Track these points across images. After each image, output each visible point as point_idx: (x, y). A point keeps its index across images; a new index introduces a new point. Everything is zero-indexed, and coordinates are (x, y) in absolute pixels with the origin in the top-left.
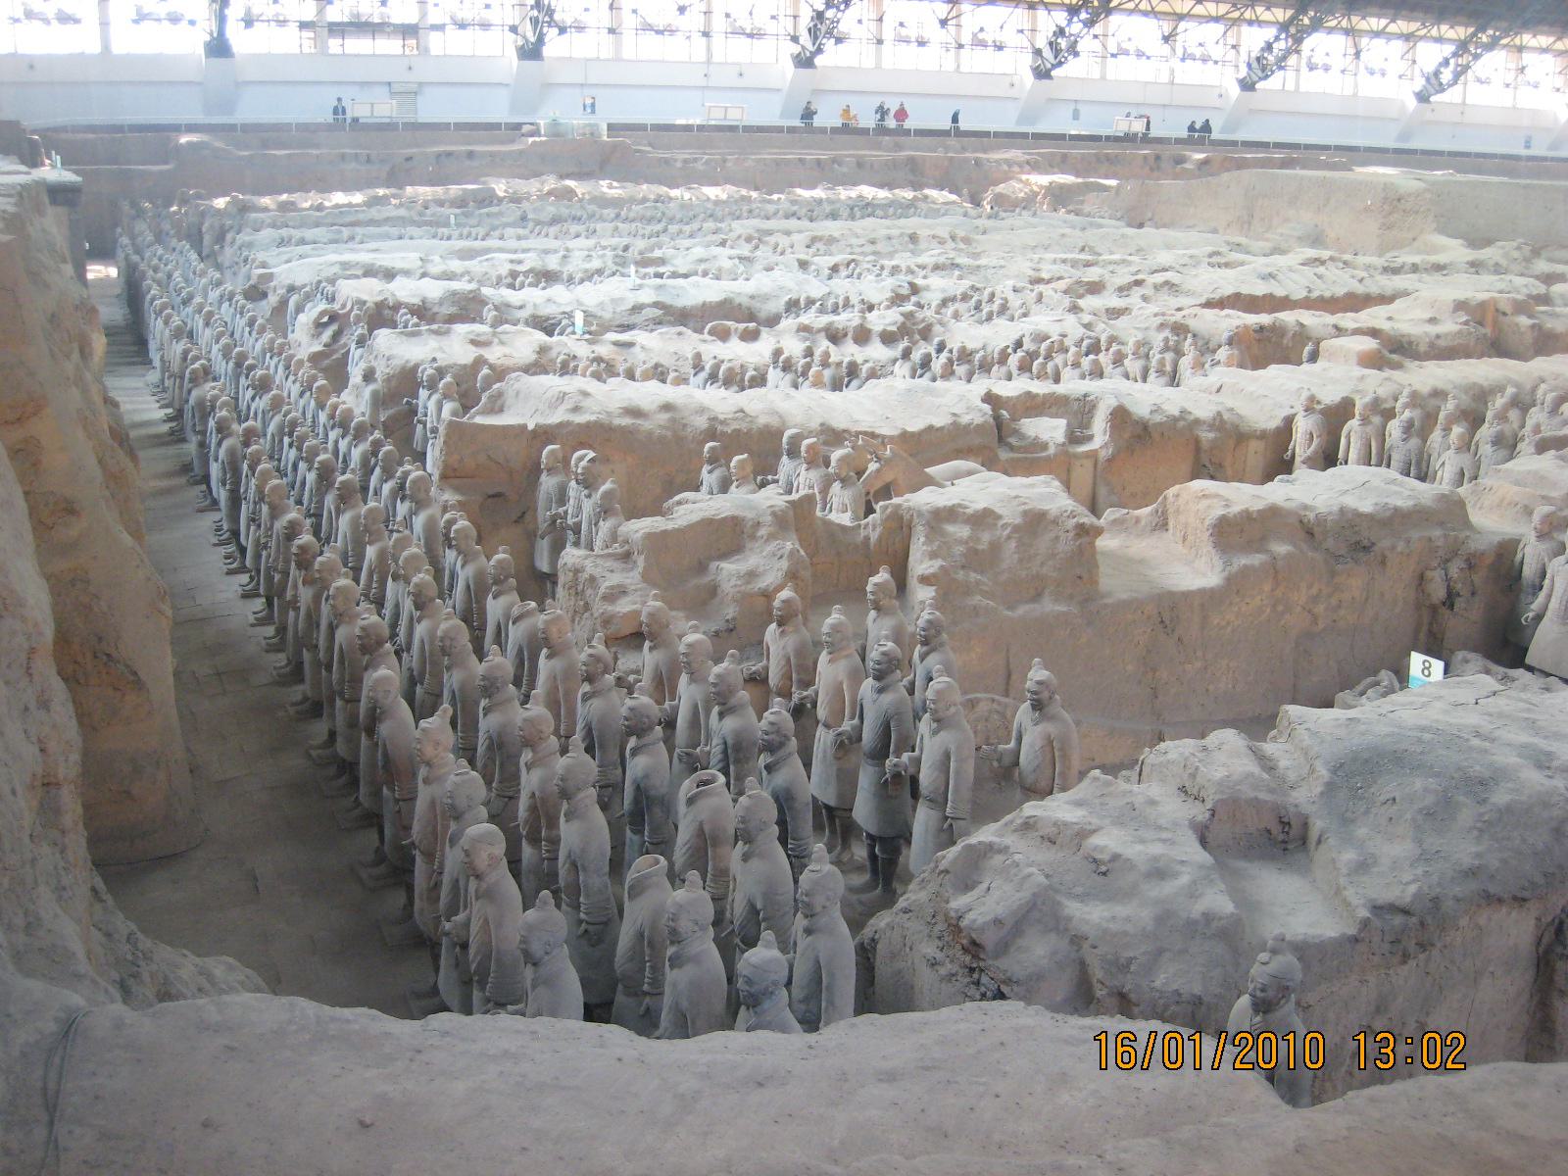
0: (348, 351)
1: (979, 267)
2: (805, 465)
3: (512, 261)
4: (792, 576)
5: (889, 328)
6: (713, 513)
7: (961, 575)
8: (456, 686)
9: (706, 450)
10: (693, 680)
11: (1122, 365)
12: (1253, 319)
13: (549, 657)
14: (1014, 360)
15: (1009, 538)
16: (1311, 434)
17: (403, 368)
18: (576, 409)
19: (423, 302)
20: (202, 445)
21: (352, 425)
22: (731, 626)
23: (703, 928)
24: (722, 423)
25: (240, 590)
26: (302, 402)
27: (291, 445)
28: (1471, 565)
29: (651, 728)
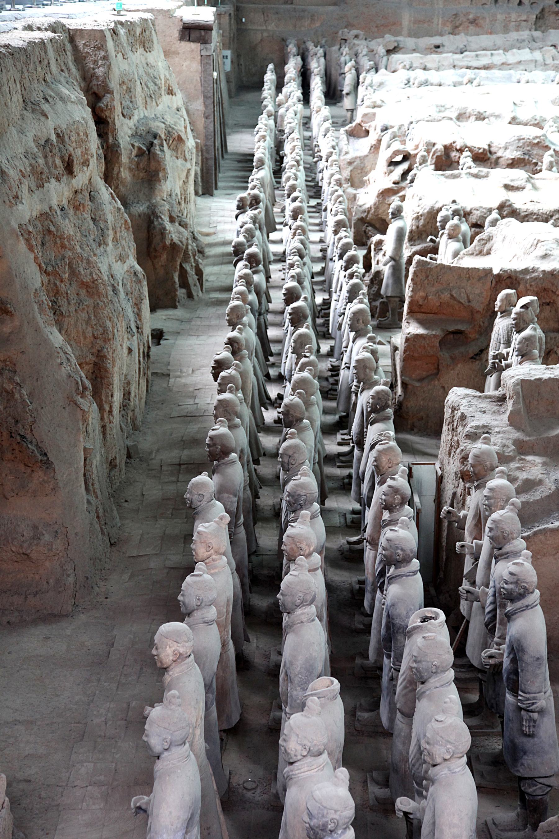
18: (545, 256)
29: (406, 560)
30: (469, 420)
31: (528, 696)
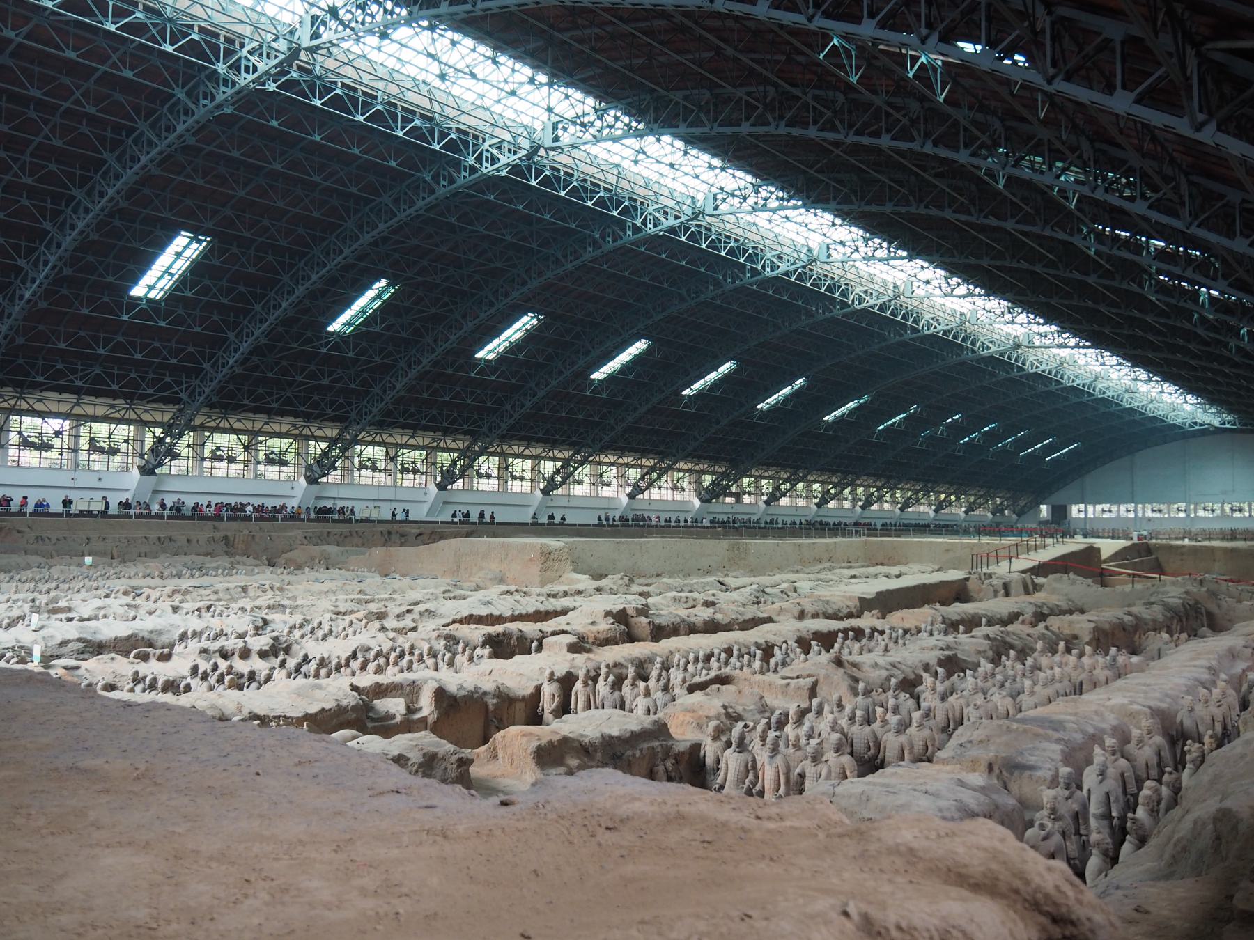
12: (492, 630)
28: (678, 757)
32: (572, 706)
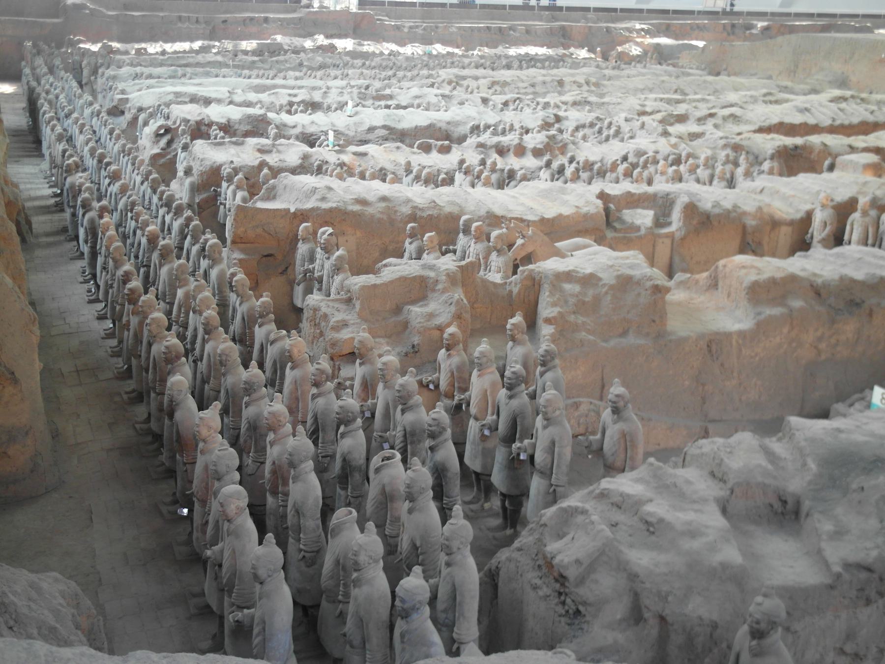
0: (177, 154)
1: (603, 103)
2: (474, 240)
3: (290, 95)
4: (458, 317)
5: (538, 146)
6: (407, 273)
7: (572, 318)
8: (229, 387)
9: (408, 228)
10: (385, 387)
11: (695, 173)
13: (292, 368)
14: (622, 168)
15: (606, 293)
16: (825, 223)
17: (212, 167)
18: (323, 199)
19: (228, 121)
20: (74, 215)
21: (174, 205)
22: (416, 350)
23: (376, 561)
24: (422, 210)
25: (96, 314)
26: (143, 188)
27: (132, 218)
29: (354, 420)
30: (331, 317)
31: (451, 499)
32: (846, 237)
